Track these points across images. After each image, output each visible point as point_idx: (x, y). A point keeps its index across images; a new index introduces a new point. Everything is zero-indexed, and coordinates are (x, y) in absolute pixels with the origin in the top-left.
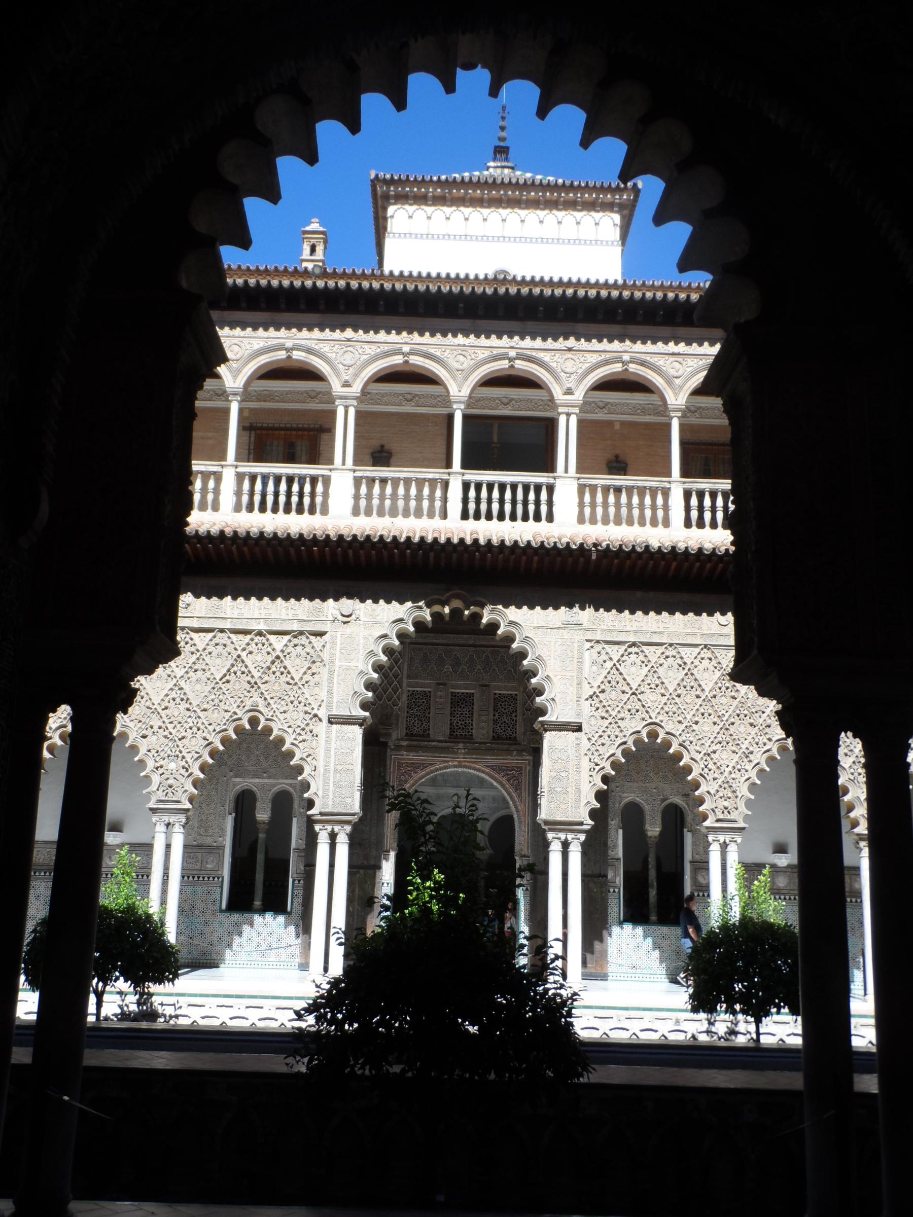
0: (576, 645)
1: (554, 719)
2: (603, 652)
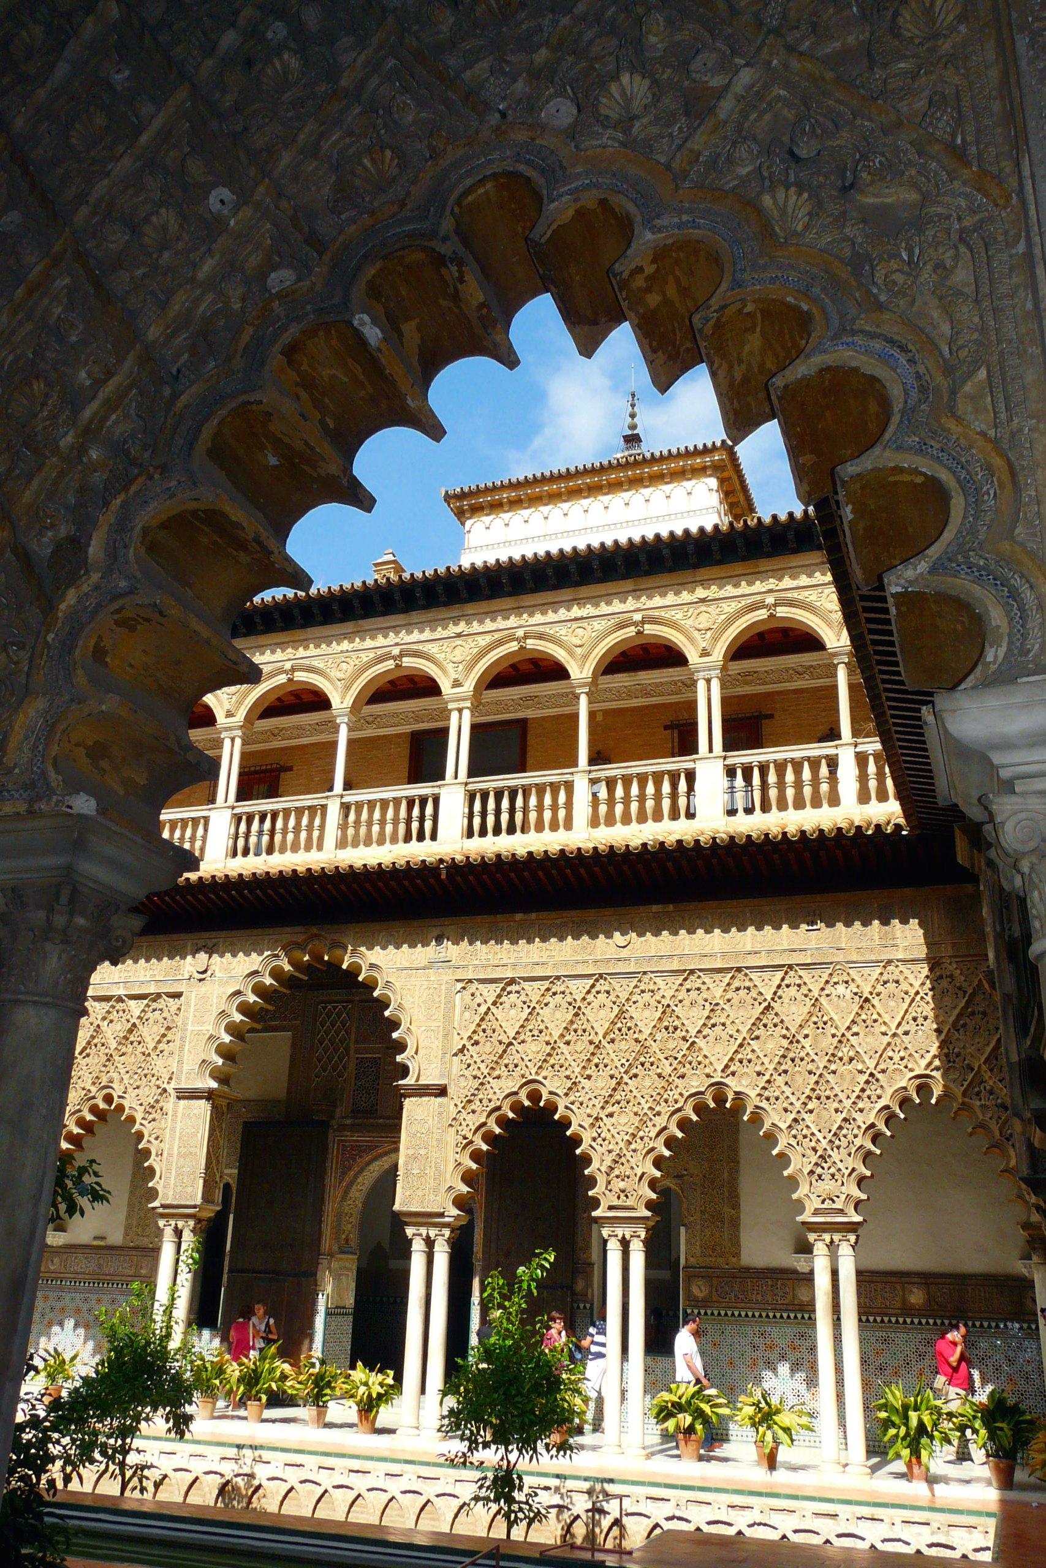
0: (443, 987)
1: (412, 1082)
2: (477, 993)
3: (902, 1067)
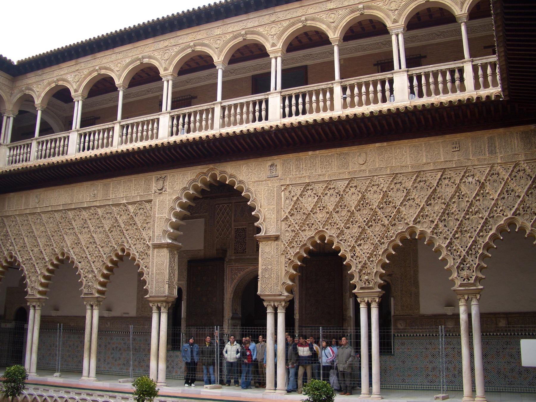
0: (275, 189)
1: (263, 235)
3: (501, 215)
